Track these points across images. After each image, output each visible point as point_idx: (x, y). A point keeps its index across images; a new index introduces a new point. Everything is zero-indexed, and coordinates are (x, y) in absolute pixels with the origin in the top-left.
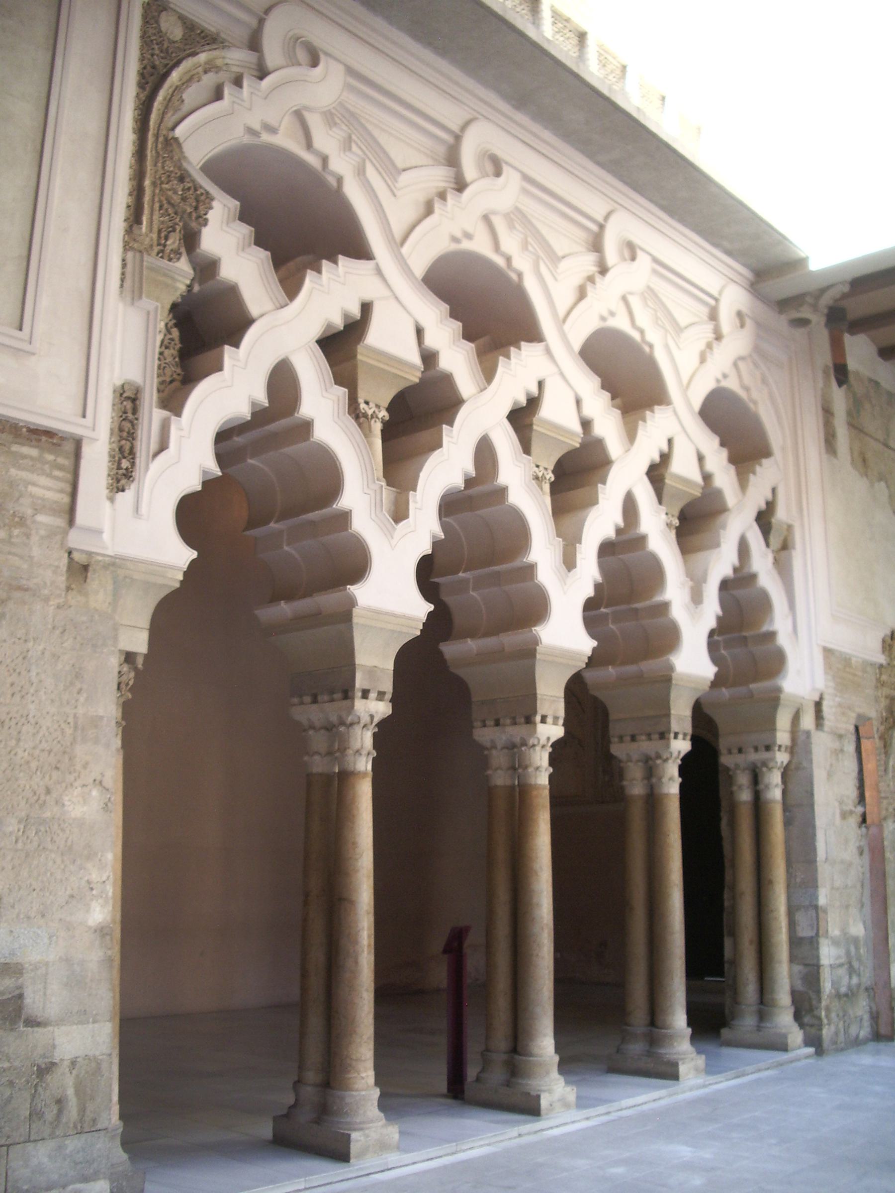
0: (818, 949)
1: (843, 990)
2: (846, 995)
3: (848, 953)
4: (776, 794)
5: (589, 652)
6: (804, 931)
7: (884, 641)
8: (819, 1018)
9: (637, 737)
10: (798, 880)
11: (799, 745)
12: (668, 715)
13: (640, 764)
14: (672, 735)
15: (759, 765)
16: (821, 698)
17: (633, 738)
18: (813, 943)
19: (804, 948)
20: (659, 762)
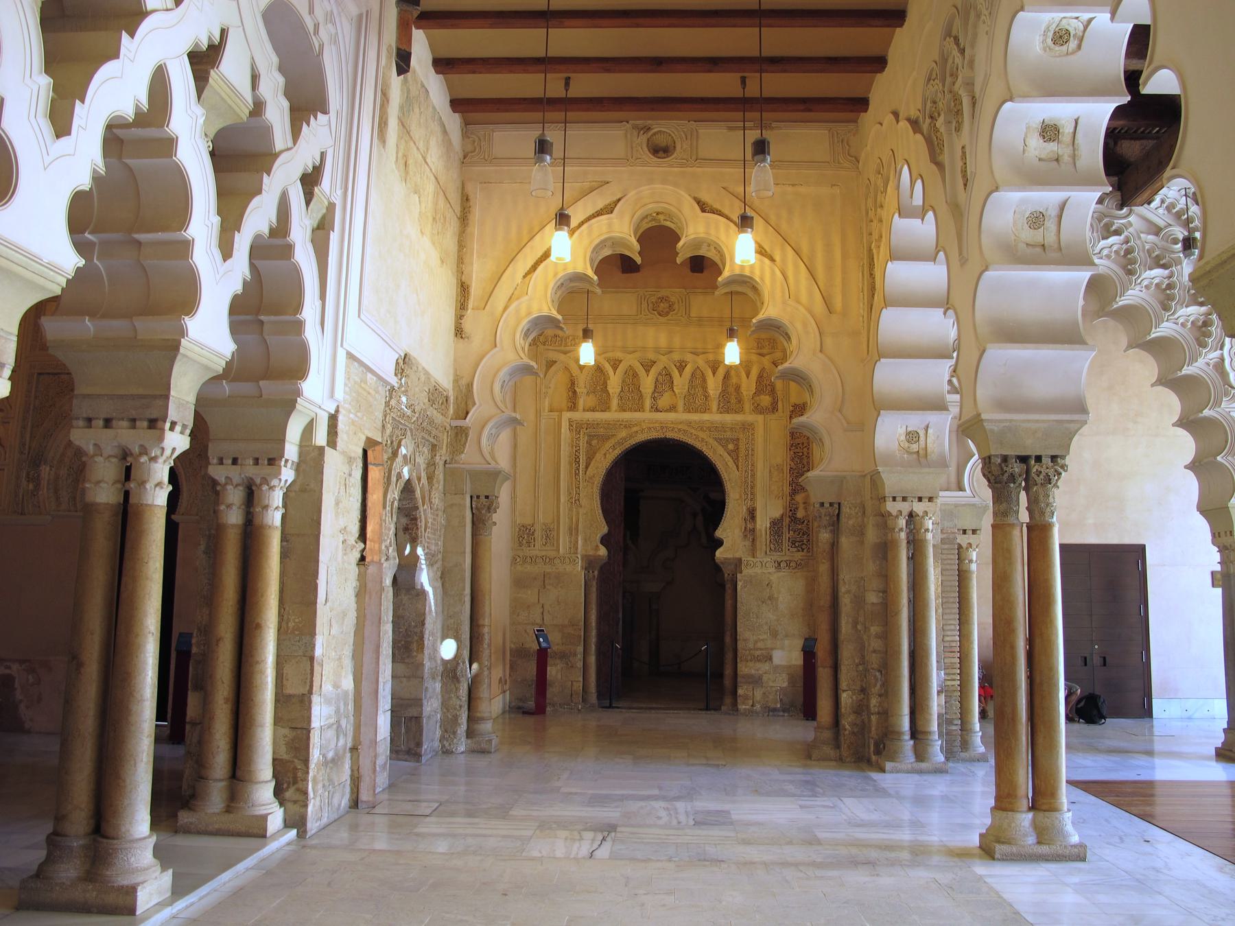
0: (310, 708)
1: (330, 755)
2: (333, 760)
3: (337, 711)
4: (275, 518)
5: (70, 272)
6: (292, 689)
7: (397, 363)
8: (306, 793)
9: (114, 422)
10: (291, 625)
11: (312, 462)
12: (166, 397)
13: (114, 460)
14: (168, 425)
15: (258, 481)
16: (337, 411)
17: (108, 423)
18: (304, 701)
19: (295, 709)
20: (144, 459)
